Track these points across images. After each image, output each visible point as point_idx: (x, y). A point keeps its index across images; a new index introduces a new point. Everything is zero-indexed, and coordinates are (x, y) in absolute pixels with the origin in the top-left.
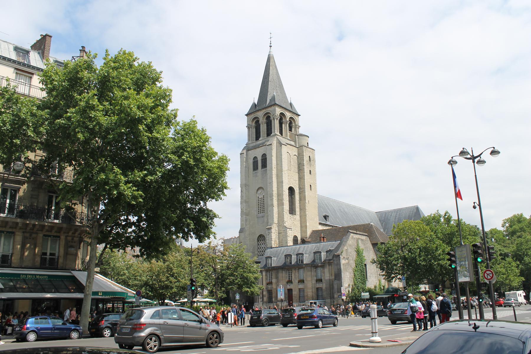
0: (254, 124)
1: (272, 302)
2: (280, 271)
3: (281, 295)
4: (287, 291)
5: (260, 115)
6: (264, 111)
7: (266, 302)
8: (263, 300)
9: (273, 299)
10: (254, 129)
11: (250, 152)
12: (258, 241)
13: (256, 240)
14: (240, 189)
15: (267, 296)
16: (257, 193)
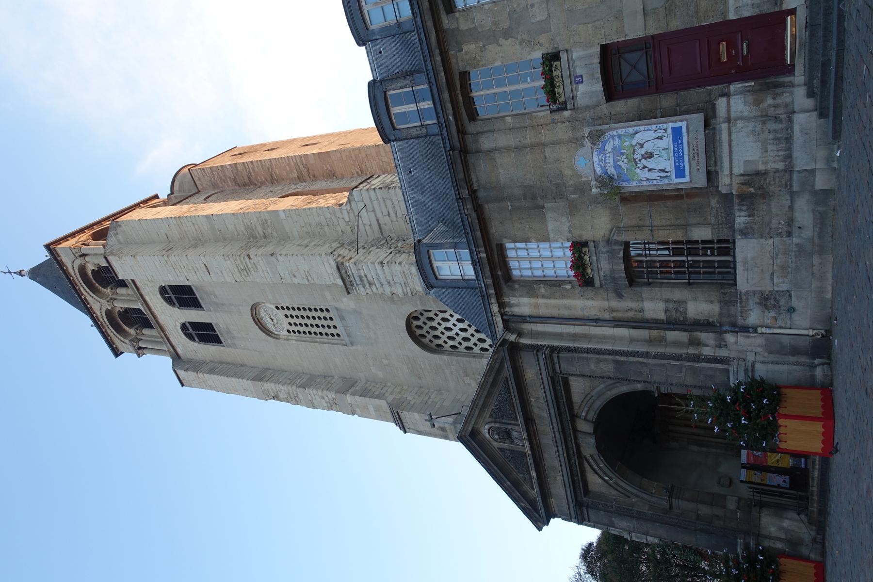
0: (132, 331)
1: (726, 247)
2: (482, 171)
3: (652, 150)
4: (620, 106)
5: (99, 305)
6: (84, 293)
7: (726, 303)
8: (706, 325)
9: (701, 233)
10: (146, 331)
11: (179, 351)
12: (438, 349)
13: (435, 358)
14: (272, 402)
15: (677, 294)
16: (276, 337)
